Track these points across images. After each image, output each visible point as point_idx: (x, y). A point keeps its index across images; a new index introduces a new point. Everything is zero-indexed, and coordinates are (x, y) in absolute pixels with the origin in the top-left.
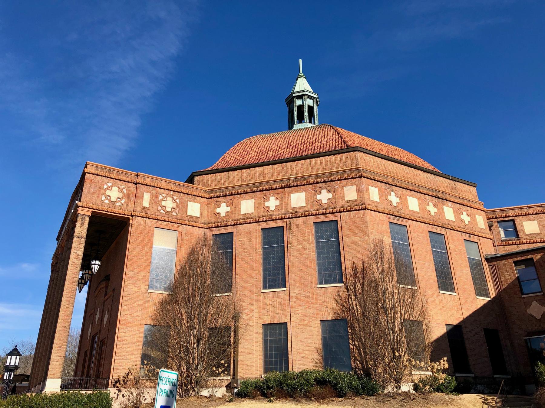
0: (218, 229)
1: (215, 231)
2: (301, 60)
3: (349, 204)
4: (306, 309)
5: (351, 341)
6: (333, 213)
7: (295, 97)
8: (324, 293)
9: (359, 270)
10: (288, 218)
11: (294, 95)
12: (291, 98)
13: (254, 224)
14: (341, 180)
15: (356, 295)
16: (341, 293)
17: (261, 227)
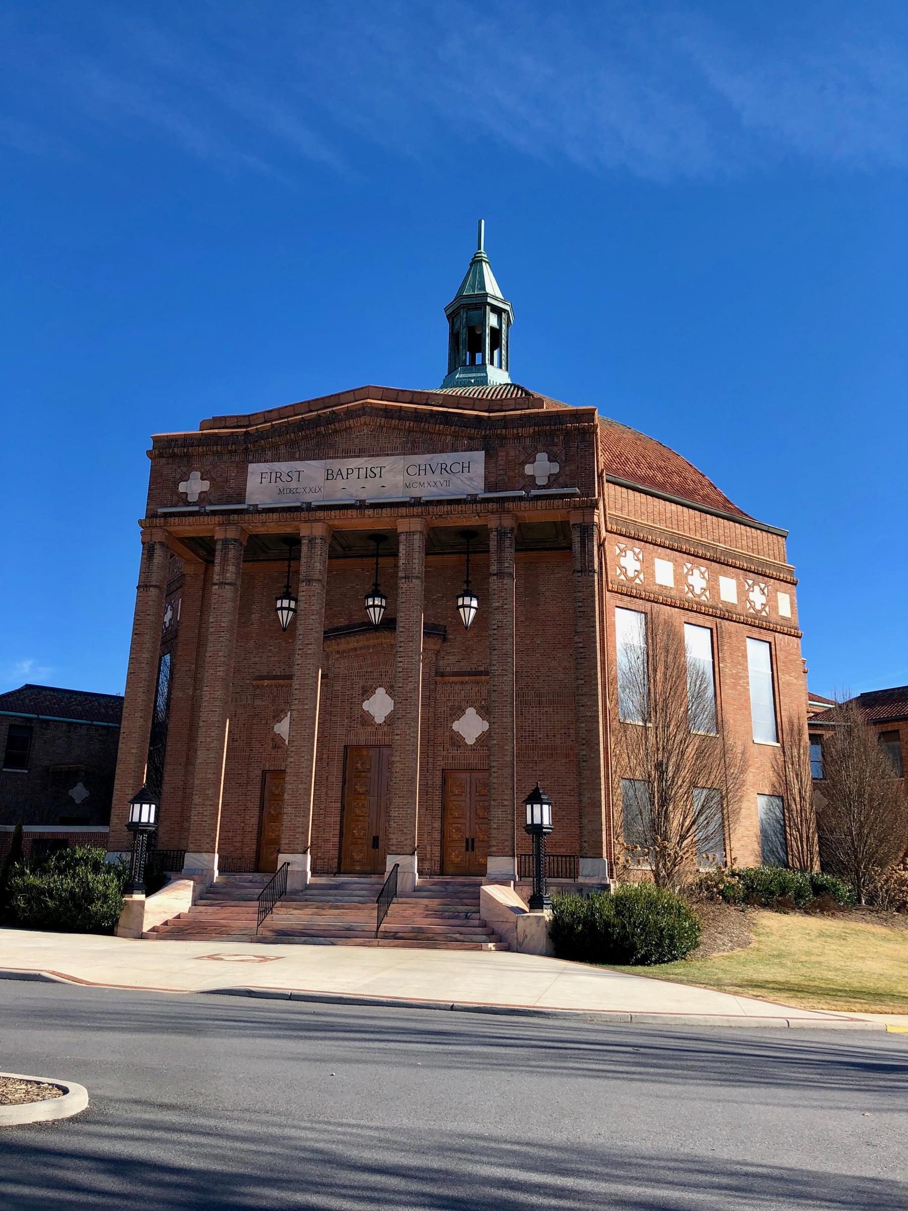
1: (621, 600)
2: (483, 221)
3: (784, 622)
5: (788, 829)
6: (768, 630)
9: (796, 728)
10: (719, 617)
11: (489, 300)
12: (479, 300)
13: (676, 609)
14: (775, 579)
15: (792, 764)
16: (778, 756)
17: (684, 619)
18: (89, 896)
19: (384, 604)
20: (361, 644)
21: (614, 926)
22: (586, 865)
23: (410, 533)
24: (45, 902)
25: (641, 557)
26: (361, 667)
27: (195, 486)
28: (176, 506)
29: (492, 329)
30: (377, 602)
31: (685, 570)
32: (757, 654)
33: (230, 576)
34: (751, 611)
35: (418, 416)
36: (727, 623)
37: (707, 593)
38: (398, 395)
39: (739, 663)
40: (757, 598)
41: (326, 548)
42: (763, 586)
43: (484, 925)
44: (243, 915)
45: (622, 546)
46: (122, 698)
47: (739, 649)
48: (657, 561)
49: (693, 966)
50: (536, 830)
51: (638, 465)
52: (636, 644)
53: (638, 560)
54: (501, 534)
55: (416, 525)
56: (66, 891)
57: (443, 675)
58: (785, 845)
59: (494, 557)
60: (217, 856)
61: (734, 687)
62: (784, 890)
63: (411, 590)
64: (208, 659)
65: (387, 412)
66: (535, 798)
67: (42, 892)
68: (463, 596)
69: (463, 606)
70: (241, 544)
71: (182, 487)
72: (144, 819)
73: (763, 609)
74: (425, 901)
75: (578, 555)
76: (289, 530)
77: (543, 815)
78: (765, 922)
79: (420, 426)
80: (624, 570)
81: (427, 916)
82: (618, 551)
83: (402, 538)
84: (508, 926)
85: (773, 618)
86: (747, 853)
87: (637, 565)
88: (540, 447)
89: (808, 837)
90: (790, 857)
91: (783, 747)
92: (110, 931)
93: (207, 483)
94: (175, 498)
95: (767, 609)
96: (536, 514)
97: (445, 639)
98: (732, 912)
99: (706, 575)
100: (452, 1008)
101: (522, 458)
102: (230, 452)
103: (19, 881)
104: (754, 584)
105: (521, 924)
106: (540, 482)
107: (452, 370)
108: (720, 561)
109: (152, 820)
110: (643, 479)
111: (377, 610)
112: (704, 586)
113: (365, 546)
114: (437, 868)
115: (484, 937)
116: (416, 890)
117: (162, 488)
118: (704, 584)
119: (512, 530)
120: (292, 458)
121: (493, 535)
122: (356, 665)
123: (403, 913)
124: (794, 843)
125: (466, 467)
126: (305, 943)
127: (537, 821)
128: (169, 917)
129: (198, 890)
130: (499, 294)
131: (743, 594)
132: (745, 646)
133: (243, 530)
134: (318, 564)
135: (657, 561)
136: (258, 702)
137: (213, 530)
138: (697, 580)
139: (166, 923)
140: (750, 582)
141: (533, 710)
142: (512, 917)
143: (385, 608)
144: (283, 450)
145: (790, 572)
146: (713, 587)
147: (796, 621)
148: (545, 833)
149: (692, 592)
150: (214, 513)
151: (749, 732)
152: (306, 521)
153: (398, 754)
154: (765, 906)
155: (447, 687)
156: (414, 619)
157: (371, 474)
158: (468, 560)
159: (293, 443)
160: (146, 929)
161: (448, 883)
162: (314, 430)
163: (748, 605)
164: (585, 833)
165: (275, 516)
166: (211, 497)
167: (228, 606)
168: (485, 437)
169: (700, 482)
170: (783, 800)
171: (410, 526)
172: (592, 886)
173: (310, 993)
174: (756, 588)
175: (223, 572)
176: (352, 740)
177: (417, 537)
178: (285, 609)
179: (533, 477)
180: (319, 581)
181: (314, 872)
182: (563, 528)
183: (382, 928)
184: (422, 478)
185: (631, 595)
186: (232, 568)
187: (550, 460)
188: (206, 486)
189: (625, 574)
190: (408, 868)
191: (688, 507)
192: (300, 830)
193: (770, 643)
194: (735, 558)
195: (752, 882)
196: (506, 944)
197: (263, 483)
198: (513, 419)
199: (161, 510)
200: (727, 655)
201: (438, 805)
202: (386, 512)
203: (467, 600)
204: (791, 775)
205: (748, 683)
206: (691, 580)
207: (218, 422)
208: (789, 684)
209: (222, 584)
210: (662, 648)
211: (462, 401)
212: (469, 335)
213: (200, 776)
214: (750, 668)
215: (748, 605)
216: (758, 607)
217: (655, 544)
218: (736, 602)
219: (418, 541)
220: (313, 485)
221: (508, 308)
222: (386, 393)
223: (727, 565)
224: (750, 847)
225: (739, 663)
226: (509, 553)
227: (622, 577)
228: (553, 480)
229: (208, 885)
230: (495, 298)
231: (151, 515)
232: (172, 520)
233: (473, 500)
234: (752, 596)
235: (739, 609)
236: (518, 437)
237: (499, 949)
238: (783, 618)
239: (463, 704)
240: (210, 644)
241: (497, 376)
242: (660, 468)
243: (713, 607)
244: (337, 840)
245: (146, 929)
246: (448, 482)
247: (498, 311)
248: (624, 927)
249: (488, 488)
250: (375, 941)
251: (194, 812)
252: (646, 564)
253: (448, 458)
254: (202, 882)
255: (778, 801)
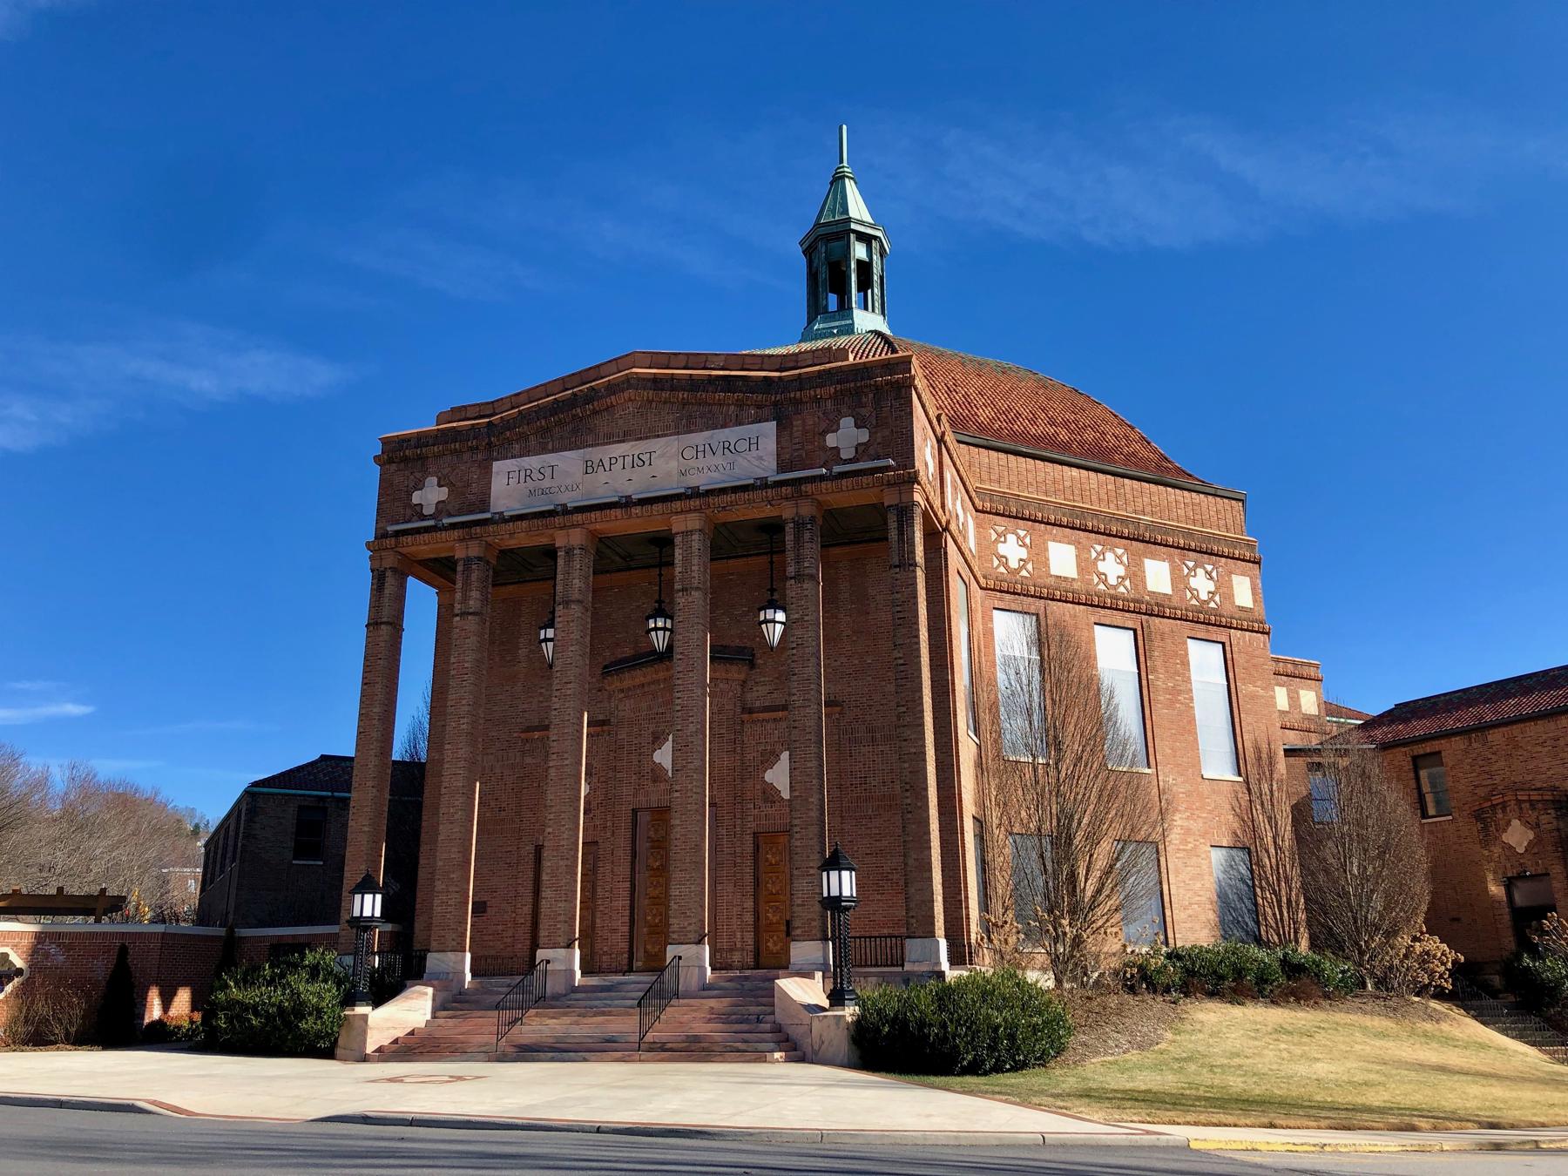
0: (1007, 596)
1: (1001, 599)
3: (1244, 615)
4: (1188, 818)
7: (854, 231)
8: (1214, 791)
9: (1264, 756)
11: (853, 226)
12: (840, 228)
18: (299, 1010)
19: (669, 625)
20: (649, 679)
21: (931, 1025)
22: (913, 947)
23: (687, 533)
24: (249, 1020)
25: (1028, 541)
26: (650, 708)
27: (431, 495)
28: (409, 521)
29: (859, 262)
30: (660, 624)
31: (1094, 555)
32: (1204, 662)
33: (474, 604)
34: (1194, 602)
35: (693, 384)
36: (1157, 620)
37: (1127, 583)
38: (667, 360)
39: (1177, 673)
40: (1202, 584)
41: (589, 560)
42: (1209, 568)
43: (778, 1029)
44: (483, 1027)
45: (1000, 529)
46: (351, 759)
47: (1176, 654)
48: (1052, 546)
49: (1062, 1076)
50: (834, 904)
51: (1033, 421)
52: (1017, 654)
53: (1024, 545)
54: (799, 525)
55: (693, 522)
56: (273, 1005)
57: (751, 711)
58: (1256, 911)
59: (790, 555)
60: (468, 956)
61: (1171, 704)
62: (1239, 973)
63: (692, 603)
64: (450, 710)
65: (656, 382)
66: (834, 863)
67: (245, 1007)
68: (764, 608)
69: (766, 621)
70: (488, 563)
71: (416, 498)
72: (367, 913)
73: (1212, 599)
74: (713, 1003)
75: (895, 545)
76: (545, 541)
77: (844, 884)
78: (1200, 1016)
79: (700, 395)
80: (1003, 560)
81: (709, 1021)
82: (994, 536)
83: (678, 540)
84: (801, 1030)
85: (1227, 610)
86: (1197, 927)
87: (1023, 553)
88: (844, 410)
89: (1289, 901)
90: (1263, 928)
91: (1247, 782)
92: (329, 1054)
93: (445, 489)
94: (409, 512)
95: (1217, 598)
96: (843, 497)
97: (752, 665)
98: (1158, 1004)
99: (1125, 559)
100: (598, 1130)
101: (823, 426)
102: (471, 449)
103: (221, 996)
104: (1196, 566)
105: (816, 1026)
106: (844, 456)
107: (811, 321)
108: (1145, 539)
109: (378, 914)
110: (1038, 440)
111: (660, 633)
112: (1122, 573)
113: (633, 554)
114: (750, 960)
115: (772, 1045)
116: (706, 989)
117: (393, 500)
118: (1121, 571)
119: (813, 518)
120: (544, 450)
121: (789, 528)
122: (644, 705)
123: (682, 1018)
124: (1268, 910)
125: (754, 443)
126: (552, 1060)
127: (835, 892)
128: (401, 1033)
129: (438, 1001)
130: (868, 218)
131: (1179, 580)
132: (1186, 650)
133: (488, 545)
134: (576, 581)
135: (1052, 546)
136: (528, 760)
137: (452, 549)
138: (1112, 567)
139: (396, 1041)
140: (1191, 564)
141: (863, 750)
142: (806, 1016)
143: (671, 630)
144: (533, 441)
145: (1250, 546)
146: (1135, 574)
147: (1260, 612)
148: (848, 909)
149: (1105, 582)
150: (453, 526)
151: (1196, 764)
152: (561, 528)
153: (677, 815)
154: (1212, 995)
155: (748, 726)
156: (699, 644)
157: (639, 462)
158: (772, 562)
159: (545, 431)
160: (370, 1049)
161: (747, 978)
162: (569, 413)
163: (1189, 595)
164: (912, 905)
165: (524, 524)
166: (449, 507)
167: (472, 641)
168: (775, 404)
169: (1126, 437)
170: (1249, 853)
171: (686, 523)
172: (921, 975)
173: (434, 1117)
174: (1200, 571)
175: (465, 599)
176: (642, 800)
177: (696, 537)
178: (551, 640)
179: (837, 449)
180: (579, 601)
181: (583, 974)
182: (880, 510)
183: (649, 1037)
184: (701, 463)
185: (1011, 591)
186: (475, 594)
187: (857, 426)
188: (443, 494)
189: (1006, 565)
190: (696, 960)
191: (1096, 470)
192: (562, 918)
193: (1223, 644)
194: (1166, 532)
195: (1193, 964)
196: (798, 1052)
197: (511, 484)
198: (810, 376)
199: (391, 528)
200: (1159, 663)
201: (749, 879)
202: (657, 508)
203: (770, 614)
204: (1261, 818)
205: (1191, 699)
206: (1102, 567)
207: (459, 412)
208: (1253, 697)
209: (463, 614)
210: (1059, 660)
211: (748, 360)
212: (830, 270)
213: (445, 856)
214: (1193, 678)
215: (1189, 595)
216: (1204, 596)
217: (1048, 523)
218: (1169, 592)
219: (696, 542)
220: (569, 481)
221: (879, 234)
222: (656, 359)
223: (1155, 543)
224: (1203, 918)
225: (1177, 673)
226: (811, 550)
227: (1002, 569)
228: (862, 451)
229: (455, 991)
230: (861, 223)
231: (381, 535)
232: (403, 539)
233: (763, 485)
234: (1193, 582)
235: (1175, 602)
236: (817, 400)
237: (789, 1060)
238: (1242, 609)
239: (778, 747)
240: (452, 691)
241: (866, 321)
242: (1066, 424)
243: (1134, 601)
244: (626, 929)
245: (370, 1049)
246: (732, 464)
247: (866, 239)
248: (944, 1026)
249: (782, 468)
250: (636, 1055)
251: (436, 902)
252: (1035, 550)
253: (730, 434)
254: (446, 988)
255: (1239, 855)
